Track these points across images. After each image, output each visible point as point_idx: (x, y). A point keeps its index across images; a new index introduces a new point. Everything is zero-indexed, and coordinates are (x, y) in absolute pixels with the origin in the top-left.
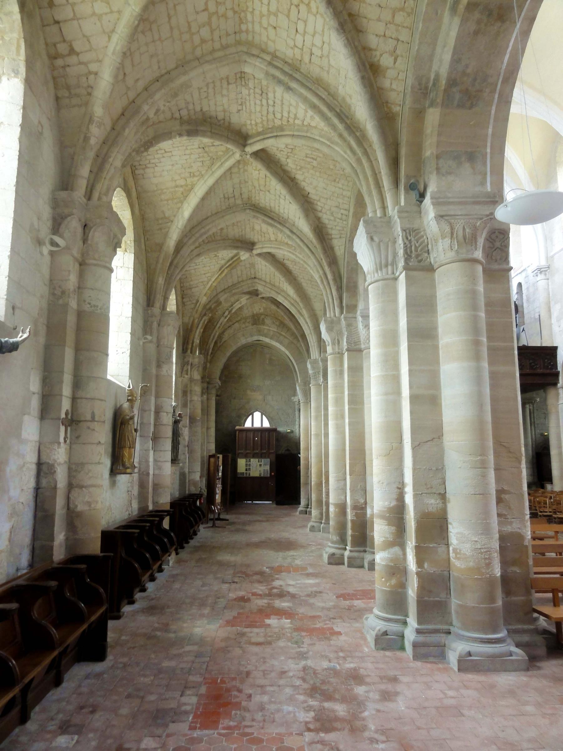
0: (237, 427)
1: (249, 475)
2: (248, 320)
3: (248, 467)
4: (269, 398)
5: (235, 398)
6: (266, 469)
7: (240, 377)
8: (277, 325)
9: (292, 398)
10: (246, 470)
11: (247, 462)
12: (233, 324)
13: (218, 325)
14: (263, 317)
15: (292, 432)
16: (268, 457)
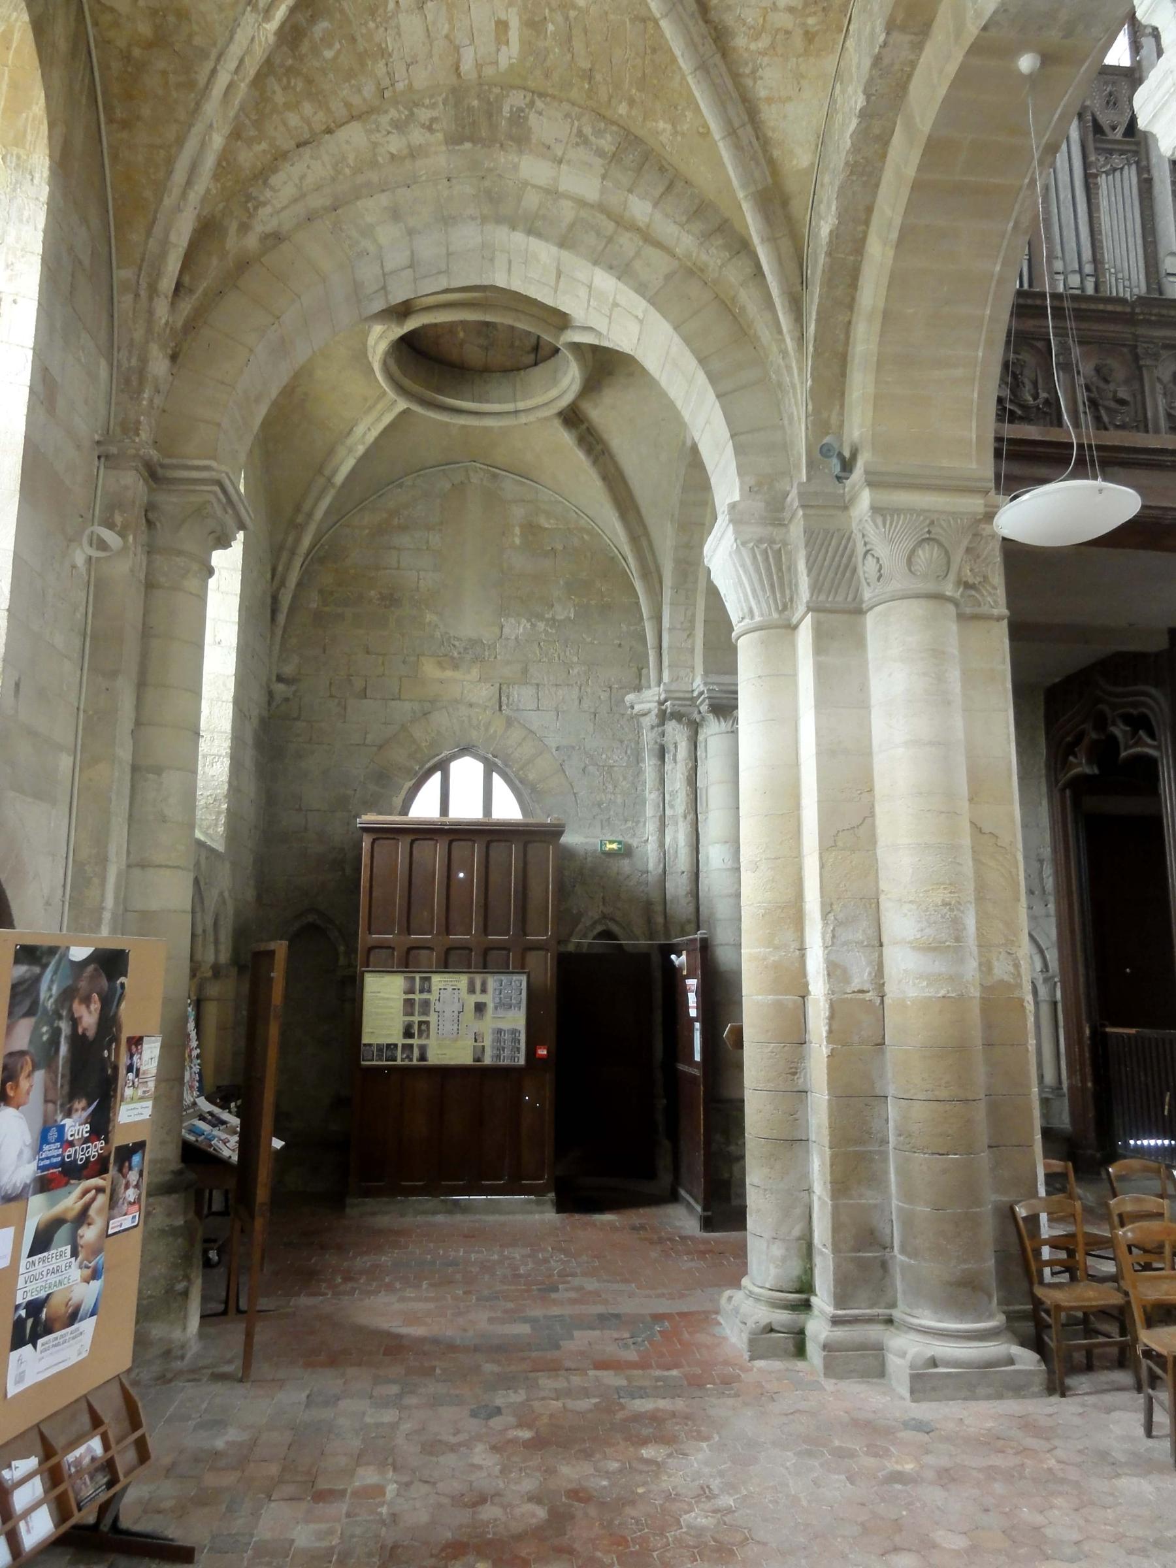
0: (370, 818)
1: (423, 1057)
2: (424, 115)
3: (416, 1019)
4: (523, 696)
5: (363, 694)
6: (505, 1026)
7: (391, 599)
8: (600, 153)
9: (630, 698)
10: (408, 1033)
11: (411, 991)
12: (329, 131)
13: (223, 80)
14: (516, 99)
15: (626, 852)
16: (521, 968)
